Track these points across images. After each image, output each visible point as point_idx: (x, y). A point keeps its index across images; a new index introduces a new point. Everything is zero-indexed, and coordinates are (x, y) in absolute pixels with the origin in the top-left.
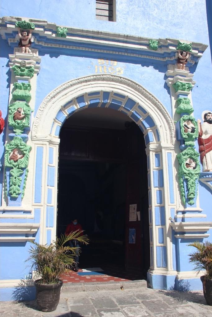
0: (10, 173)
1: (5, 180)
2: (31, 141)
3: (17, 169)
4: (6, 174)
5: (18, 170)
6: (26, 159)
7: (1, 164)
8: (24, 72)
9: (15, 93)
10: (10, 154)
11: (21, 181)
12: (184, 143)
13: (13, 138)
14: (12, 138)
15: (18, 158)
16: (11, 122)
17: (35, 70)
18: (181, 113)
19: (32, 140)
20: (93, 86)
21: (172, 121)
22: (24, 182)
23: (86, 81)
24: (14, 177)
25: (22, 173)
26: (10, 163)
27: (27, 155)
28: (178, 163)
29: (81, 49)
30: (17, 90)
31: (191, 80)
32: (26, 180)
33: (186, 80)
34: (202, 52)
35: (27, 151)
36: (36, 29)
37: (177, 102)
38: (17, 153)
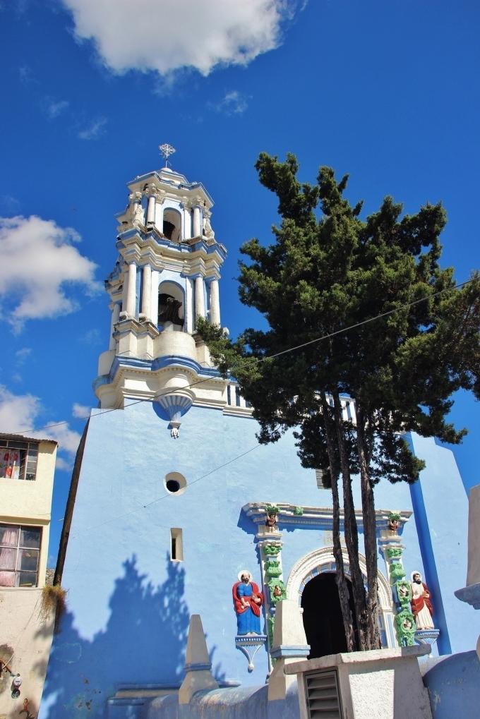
8: (274, 552)
12: (401, 606)
18: (395, 578)
20: (325, 557)
21: (389, 585)
23: (319, 554)
28: (397, 624)
29: (312, 523)
31: (401, 546)
33: (397, 547)
34: (409, 517)
36: (281, 511)
37: (391, 567)
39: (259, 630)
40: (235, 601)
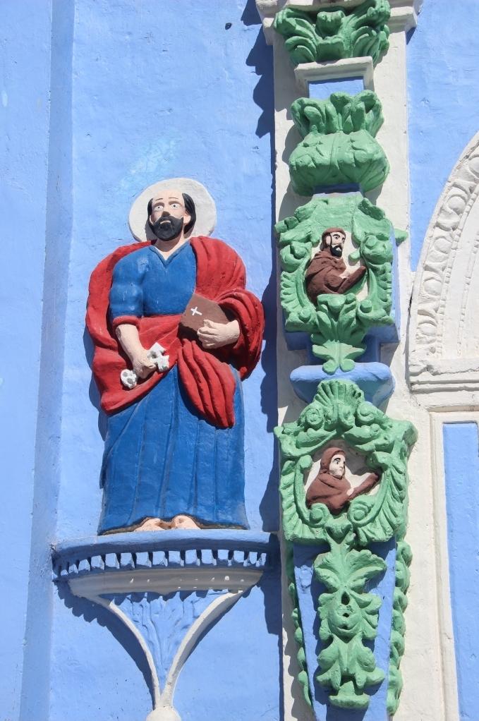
0: (315, 574)
1: (295, 615)
2: (407, 394)
3: (350, 549)
4: (292, 578)
5: (355, 552)
6: (389, 495)
7: (265, 529)
8: (340, 37)
9: (303, 155)
10: (305, 472)
11: (374, 613)
13: (316, 391)
14: (308, 391)
15: (350, 492)
16: (297, 307)
17: (396, 12)
19: (412, 392)
22: (395, 618)
24: (338, 595)
25: (380, 569)
26: (313, 523)
27: (395, 474)
30: (311, 138)
32: (404, 608)
35: (395, 452)
38: (341, 464)
39: (237, 491)
40: (92, 341)
